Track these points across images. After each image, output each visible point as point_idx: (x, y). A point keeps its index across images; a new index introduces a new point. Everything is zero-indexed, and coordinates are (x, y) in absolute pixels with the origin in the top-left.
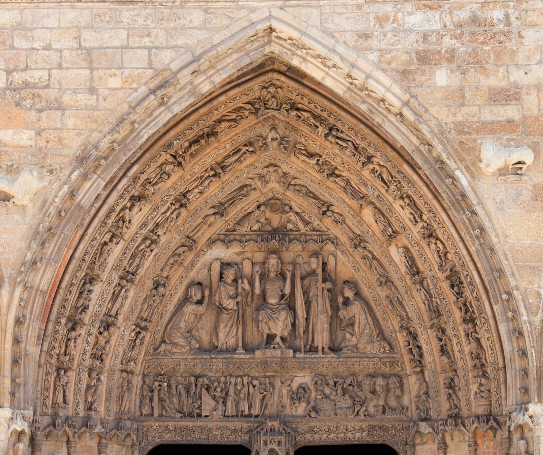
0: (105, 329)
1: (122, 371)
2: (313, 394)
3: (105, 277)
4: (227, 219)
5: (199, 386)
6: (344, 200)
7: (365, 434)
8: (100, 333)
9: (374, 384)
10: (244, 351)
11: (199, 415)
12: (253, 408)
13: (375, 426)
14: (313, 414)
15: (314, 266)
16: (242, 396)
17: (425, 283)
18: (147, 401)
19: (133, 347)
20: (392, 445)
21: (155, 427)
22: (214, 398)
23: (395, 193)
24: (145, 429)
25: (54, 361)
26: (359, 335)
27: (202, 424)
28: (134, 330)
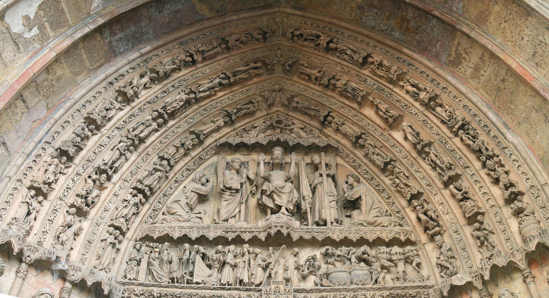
1: (110, 226)
4: (235, 127)
5: (193, 253)
9: (390, 254)
10: (246, 223)
12: (254, 276)
16: (241, 265)
19: (126, 206)
21: (137, 292)
22: (210, 267)
26: (367, 213)
28: (131, 194)
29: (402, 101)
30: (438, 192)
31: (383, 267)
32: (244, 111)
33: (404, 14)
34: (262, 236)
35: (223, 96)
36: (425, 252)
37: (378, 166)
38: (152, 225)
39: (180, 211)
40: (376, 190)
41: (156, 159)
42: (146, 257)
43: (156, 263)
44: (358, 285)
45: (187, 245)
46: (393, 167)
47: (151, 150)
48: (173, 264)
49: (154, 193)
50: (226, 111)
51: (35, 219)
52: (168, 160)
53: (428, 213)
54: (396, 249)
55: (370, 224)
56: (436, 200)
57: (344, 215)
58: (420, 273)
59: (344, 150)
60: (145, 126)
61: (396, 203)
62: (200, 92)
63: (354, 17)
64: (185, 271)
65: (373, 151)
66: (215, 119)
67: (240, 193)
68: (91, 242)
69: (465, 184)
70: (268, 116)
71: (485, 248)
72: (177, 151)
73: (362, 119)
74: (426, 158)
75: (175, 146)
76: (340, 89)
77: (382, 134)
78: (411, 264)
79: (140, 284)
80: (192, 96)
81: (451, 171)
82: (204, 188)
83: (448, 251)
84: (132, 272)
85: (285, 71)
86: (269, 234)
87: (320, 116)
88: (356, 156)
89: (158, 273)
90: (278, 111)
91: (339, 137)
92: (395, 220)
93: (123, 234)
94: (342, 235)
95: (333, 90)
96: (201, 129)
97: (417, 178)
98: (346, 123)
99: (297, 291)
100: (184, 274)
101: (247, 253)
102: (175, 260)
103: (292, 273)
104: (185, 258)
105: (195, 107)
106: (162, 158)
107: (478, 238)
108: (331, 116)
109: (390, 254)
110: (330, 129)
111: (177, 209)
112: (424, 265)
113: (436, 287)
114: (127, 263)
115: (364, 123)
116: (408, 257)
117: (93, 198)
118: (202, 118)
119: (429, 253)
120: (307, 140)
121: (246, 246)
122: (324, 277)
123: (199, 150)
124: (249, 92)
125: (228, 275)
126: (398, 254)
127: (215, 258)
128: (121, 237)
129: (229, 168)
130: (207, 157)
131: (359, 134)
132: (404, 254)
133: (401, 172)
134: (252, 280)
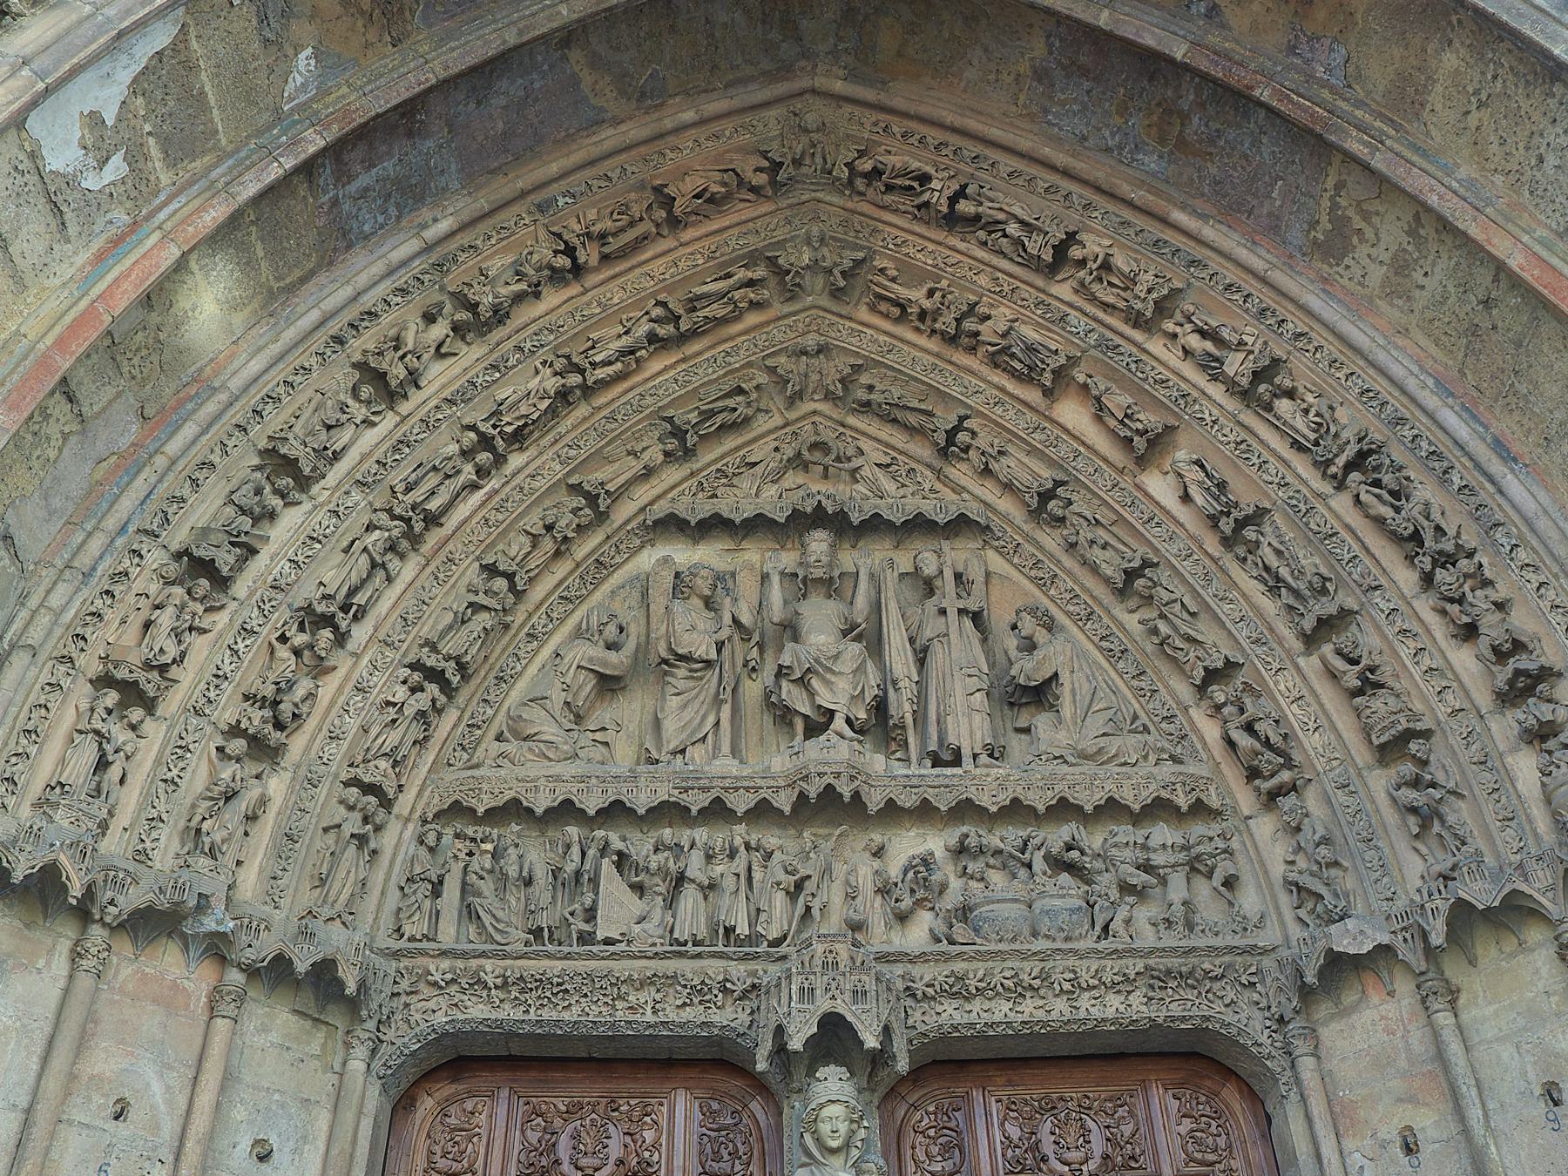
0: (301, 629)
1: (347, 784)
2: (955, 884)
3: (327, 493)
4: (695, 466)
5: (591, 853)
6: (1002, 389)
7: (1136, 999)
8: (283, 639)
9: (1145, 847)
10: (736, 762)
11: (585, 938)
12: (763, 917)
13: (1168, 972)
14: (960, 932)
15: (929, 570)
16: (729, 883)
17: (1267, 529)
18: (420, 895)
19: (394, 721)
20: (1234, 1031)
21: (437, 977)
22: (639, 889)
23: (1155, 295)
24: (405, 985)
25: (90, 664)
27: (593, 964)
28: (404, 682)
29: (1171, 383)
30: (1288, 665)
31: (1126, 888)
32: (719, 420)
33: (1170, 93)
34: (784, 802)
35: (659, 373)
36: (1248, 844)
37: (1107, 581)
38: (469, 773)
39: (550, 731)
40: (1100, 649)
41: (471, 573)
42: (457, 868)
43: (487, 887)
44: (1054, 940)
45: (573, 831)
46: (1150, 584)
47: (459, 546)
48: (535, 889)
49: (470, 676)
50: (670, 420)
51: (122, 782)
52: (510, 577)
53: (1257, 727)
54: (1162, 833)
55: (1086, 758)
56: (1282, 687)
57: (1009, 725)
58: (1237, 909)
59: (1005, 532)
60: (441, 475)
61: (1163, 690)
62: (594, 365)
63: (1024, 106)
64: (570, 909)
65: (1090, 536)
66: (638, 448)
67: (718, 669)
68: (296, 838)
69: (1368, 639)
70: (786, 430)
71: (1434, 843)
72: (534, 546)
73: (1056, 439)
74: (1250, 557)
75: (528, 533)
76: (991, 349)
77: (1114, 486)
78: (1209, 875)
79: (444, 954)
80: (574, 379)
81: (1324, 599)
82: (613, 656)
83: (1318, 845)
84: (416, 918)
85: (836, 293)
86: (802, 796)
87: (935, 431)
88: (1041, 548)
89: (494, 916)
90: (815, 412)
91: (988, 492)
92: (1159, 745)
93: (387, 803)
94: (1006, 794)
95: (972, 350)
96: (600, 476)
97: (1224, 618)
98: (1010, 448)
99: (883, 958)
100: (568, 916)
101: (742, 848)
102: (542, 875)
103: (868, 905)
104: (570, 868)
105: (582, 410)
106: (491, 570)
107: (1414, 810)
108: (967, 429)
109: (1145, 847)
110: (963, 466)
111: (541, 725)
112: (1246, 877)
113: (1284, 953)
114: (402, 888)
115: (1063, 450)
116: (1198, 857)
117: (296, 705)
118: (603, 443)
119: (1261, 845)
120: (897, 501)
121: (740, 829)
122: (956, 917)
123: (594, 540)
124: (732, 360)
125: (691, 913)
126: (1170, 849)
127: (653, 866)
128: (381, 815)
129: (683, 593)
130: (618, 559)
131: (1050, 485)
132: (1184, 848)
133: (1176, 601)
134: (759, 929)
